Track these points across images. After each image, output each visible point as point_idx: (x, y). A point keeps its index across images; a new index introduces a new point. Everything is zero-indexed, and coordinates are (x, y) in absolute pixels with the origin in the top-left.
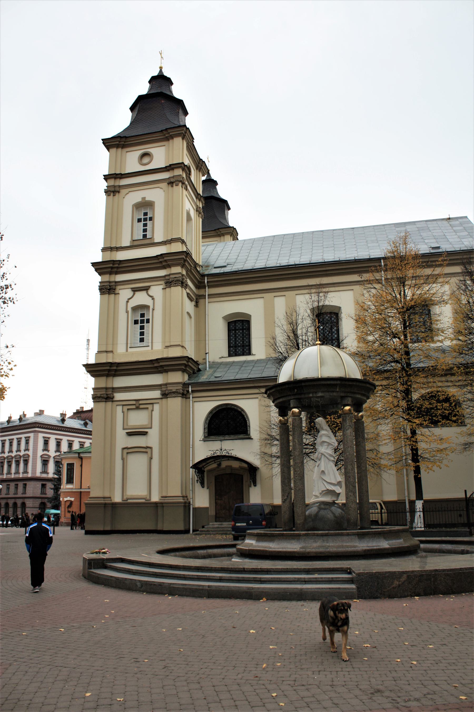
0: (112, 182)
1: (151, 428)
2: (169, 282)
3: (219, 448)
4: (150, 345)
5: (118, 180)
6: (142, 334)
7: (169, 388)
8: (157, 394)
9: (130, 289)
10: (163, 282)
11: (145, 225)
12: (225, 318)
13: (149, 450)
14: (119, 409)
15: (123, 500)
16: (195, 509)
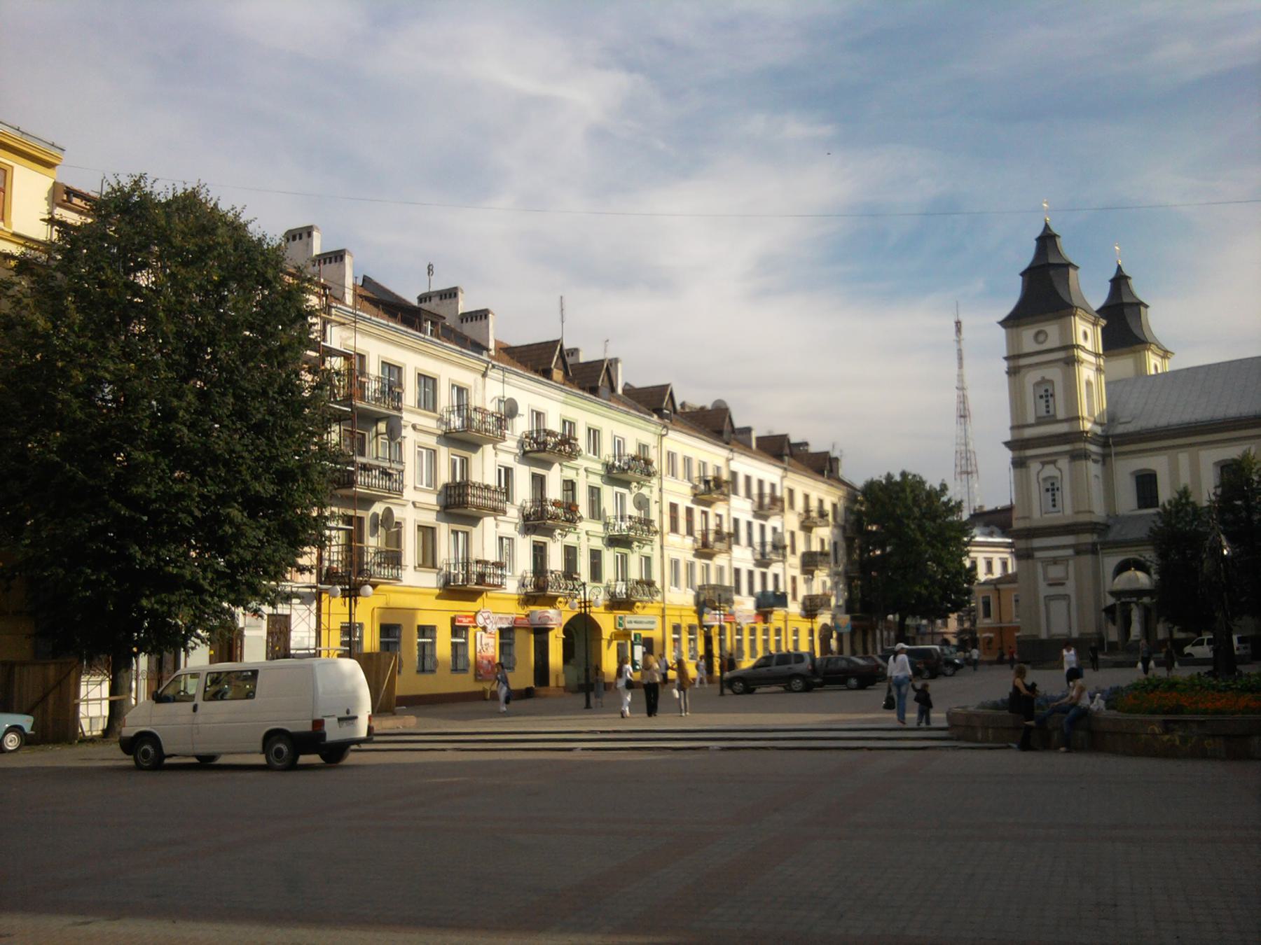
0: (1012, 363)
2: (1076, 456)
6: (1054, 500)
8: (1070, 552)
14: (1039, 565)
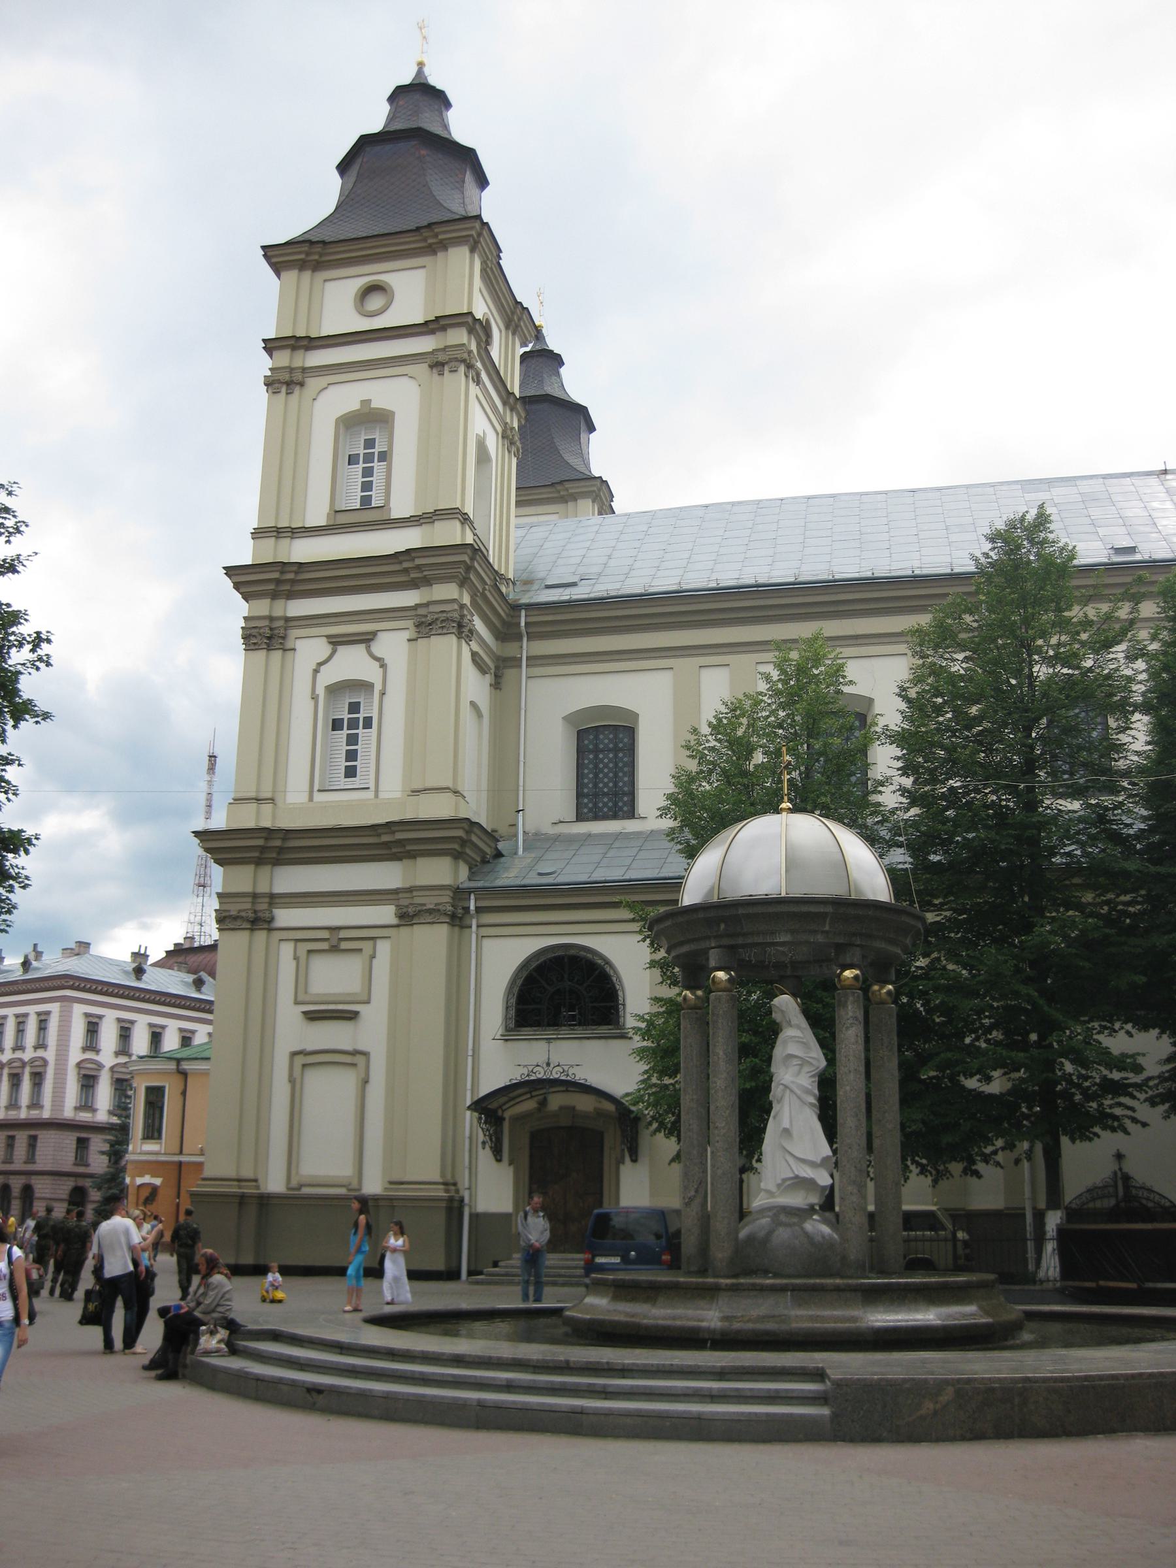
0: (283, 358)
1: (368, 1002)
2: (427, 624)
3: (542, 1060)
4: (372, 785)
5: (301, 353)
6: (351, 755)
7: (417, 900)
8: (385, 914)
9: (324, 639)
10: (409, 623)
11: (368, 472)
12: (568, 719)
13: (360, 1060)
14: (287, 950)
15: (289, 1189)
16: (475, 1217)
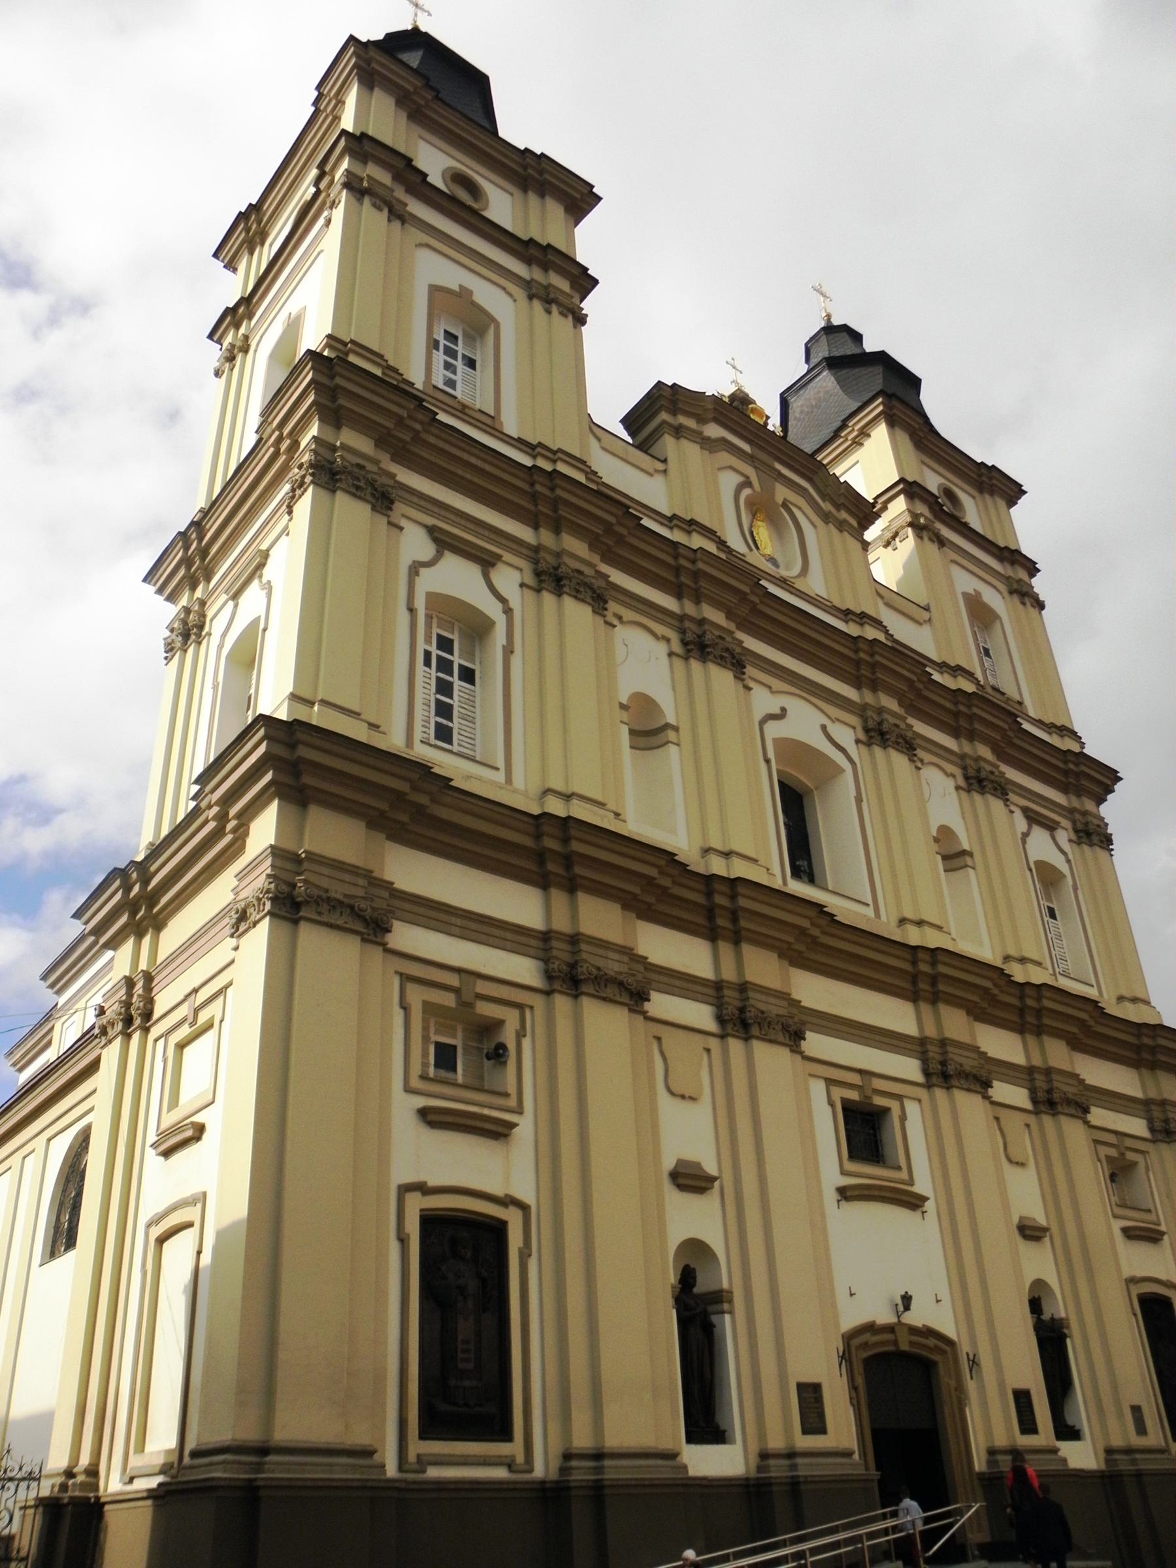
4: (501, 763)
6: (444, 710)
15: (401, 1469)
